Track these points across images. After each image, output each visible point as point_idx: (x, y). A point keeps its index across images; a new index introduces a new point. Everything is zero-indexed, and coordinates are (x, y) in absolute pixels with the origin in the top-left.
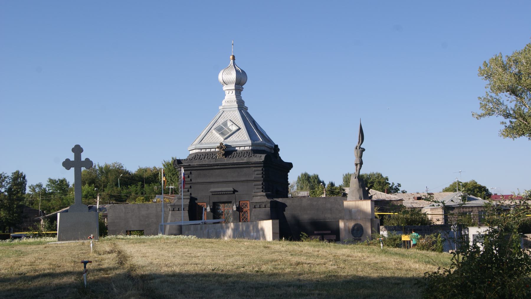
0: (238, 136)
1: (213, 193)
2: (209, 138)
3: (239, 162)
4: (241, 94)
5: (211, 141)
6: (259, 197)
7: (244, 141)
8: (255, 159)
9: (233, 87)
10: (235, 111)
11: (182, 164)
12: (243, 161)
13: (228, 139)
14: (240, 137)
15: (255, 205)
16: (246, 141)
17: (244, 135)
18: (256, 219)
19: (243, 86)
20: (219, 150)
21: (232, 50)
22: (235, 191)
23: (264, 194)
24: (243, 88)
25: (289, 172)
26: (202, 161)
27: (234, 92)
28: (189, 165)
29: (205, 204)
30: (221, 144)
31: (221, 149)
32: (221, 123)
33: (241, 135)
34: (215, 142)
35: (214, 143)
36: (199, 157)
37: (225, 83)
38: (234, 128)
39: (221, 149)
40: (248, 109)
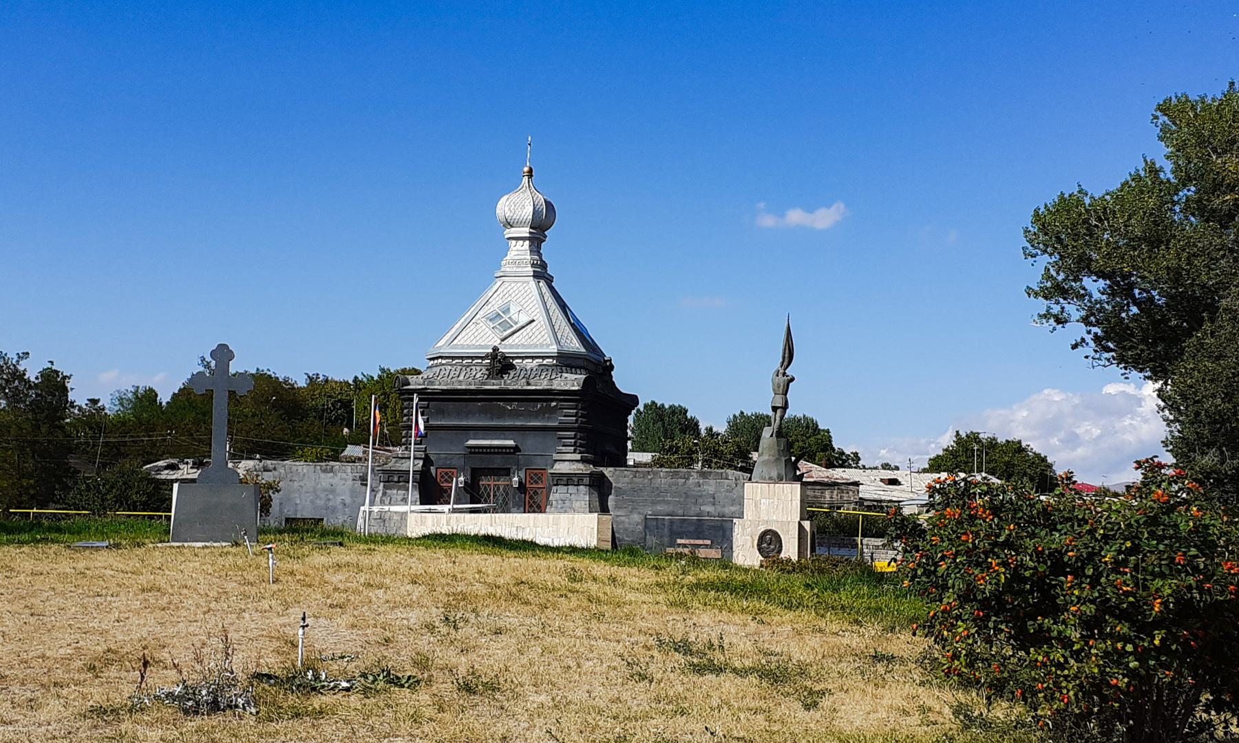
0: (531, 334)
1: (473, 450)
2: (470, 335)
5: (474, 342)
6: (567, 463)
7: (542, 346)
9: (525, 231)
12: (538, 388)
13: (510, 341)
16: (548, 346)
17: (543, 333)
19: (546, 233)
20: (489, 361)
22: (516, 449)
23: (578, 457)
24: (546, 237)
27: (527, 243)
28: (426, 389)
29: (455, 471)
30: (495, 349)
32: (496, 307)
33: (537, 332)
34: (483, 344)
35: (481, 347)
37: (509, 223)
38: (523, 319)
39: (494, 359)
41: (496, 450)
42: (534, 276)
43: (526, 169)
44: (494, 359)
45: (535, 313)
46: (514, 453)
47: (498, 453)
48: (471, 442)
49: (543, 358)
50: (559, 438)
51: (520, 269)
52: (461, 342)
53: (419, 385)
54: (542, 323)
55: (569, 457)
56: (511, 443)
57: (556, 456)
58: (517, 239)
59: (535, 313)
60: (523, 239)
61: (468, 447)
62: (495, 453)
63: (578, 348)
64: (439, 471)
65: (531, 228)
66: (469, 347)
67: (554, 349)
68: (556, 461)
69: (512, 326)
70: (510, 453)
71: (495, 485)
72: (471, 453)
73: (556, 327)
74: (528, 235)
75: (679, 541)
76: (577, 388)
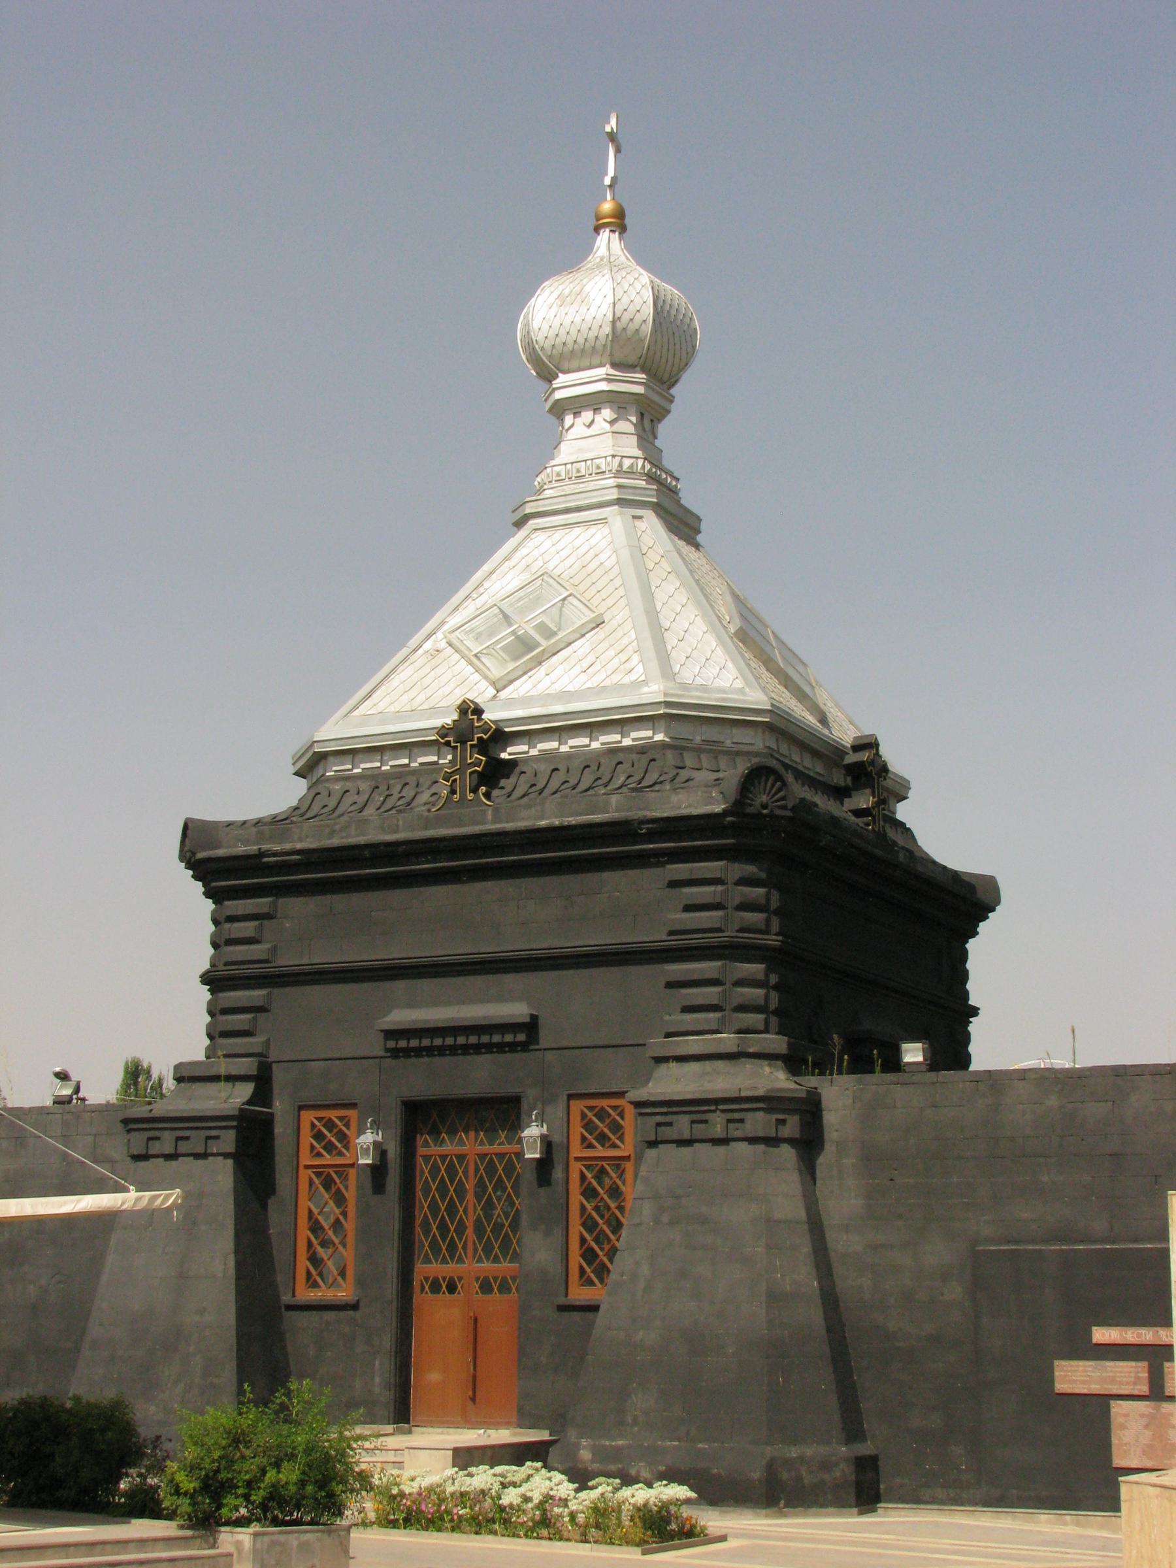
1: (403, 1044)
3: (572, 820)
4: (655, 437)
8: (674, 798)
10: (603, 521)
11: (218, 847)
14: (597, 666)
15: (659, 1119)
16: (637, 685)
18: (665, 1218)
21: (611, 172)
22: (531, 1027)
24: (671, 400)
25: (974, 934)
26: (341, 830)
28: (261, 854)
29: (352, 1114)
31: (464, 750)
36: (332, 803)
39: (463, 743)
40: (703, 526)
41: (473, 1040)
42: (620, 502)
43: (607, 206)
44: (463, 743)
45: (609, 602)
46: (524, 1047)
47: (478, 1049)
48: (401, 1017)
49: (621, 725)
50: (670, 985)
51: (581, 488)
52: (381, 706)
53: (246, 842)
54: (629, 625)
55: (693, 1045)
56: (516, 1011)
57: (658, 1045)
58: (576, 405)
59: (609, 602)
60: (593, 402)
61: (390, 1034)
62: (466, 1049)
63: (741, 691)
64: (308, 1117)
65: (615, 366)
66: (399, 716)
67: (653, 692)
68: (659, 1060)
69: (538, 645)
70: (513, 1047)
71: (482, 1156)
72: (395, 1053)
73: (671, 640)
74: (604, 386)
75: (1101, 1335)
76: (718, 808)
